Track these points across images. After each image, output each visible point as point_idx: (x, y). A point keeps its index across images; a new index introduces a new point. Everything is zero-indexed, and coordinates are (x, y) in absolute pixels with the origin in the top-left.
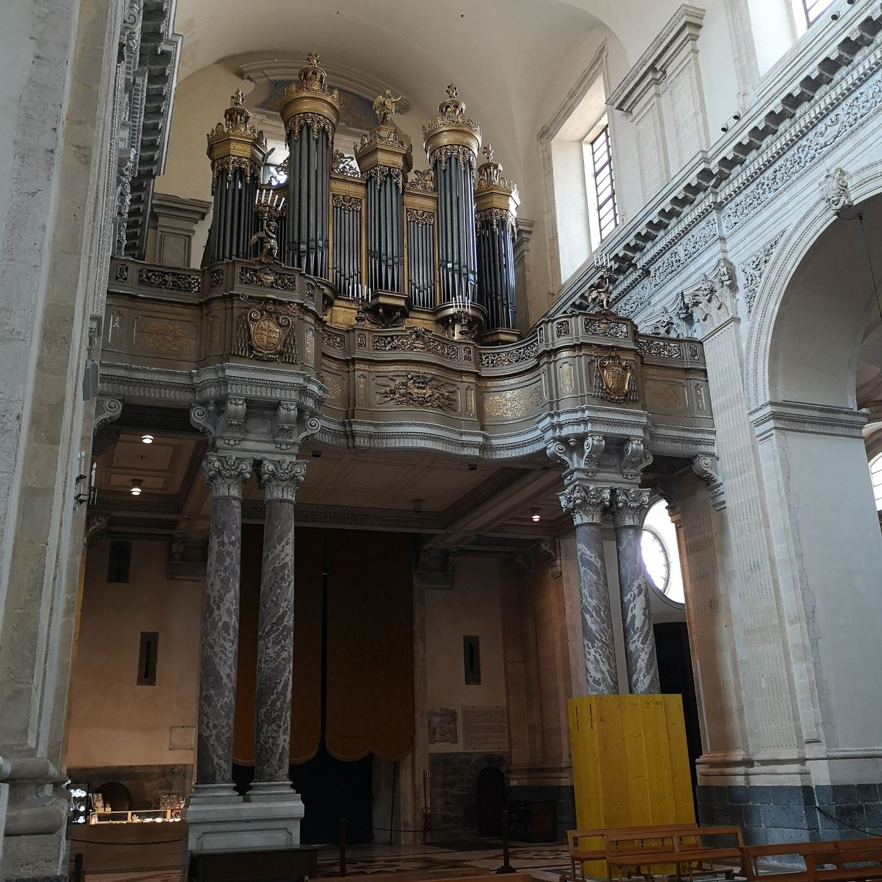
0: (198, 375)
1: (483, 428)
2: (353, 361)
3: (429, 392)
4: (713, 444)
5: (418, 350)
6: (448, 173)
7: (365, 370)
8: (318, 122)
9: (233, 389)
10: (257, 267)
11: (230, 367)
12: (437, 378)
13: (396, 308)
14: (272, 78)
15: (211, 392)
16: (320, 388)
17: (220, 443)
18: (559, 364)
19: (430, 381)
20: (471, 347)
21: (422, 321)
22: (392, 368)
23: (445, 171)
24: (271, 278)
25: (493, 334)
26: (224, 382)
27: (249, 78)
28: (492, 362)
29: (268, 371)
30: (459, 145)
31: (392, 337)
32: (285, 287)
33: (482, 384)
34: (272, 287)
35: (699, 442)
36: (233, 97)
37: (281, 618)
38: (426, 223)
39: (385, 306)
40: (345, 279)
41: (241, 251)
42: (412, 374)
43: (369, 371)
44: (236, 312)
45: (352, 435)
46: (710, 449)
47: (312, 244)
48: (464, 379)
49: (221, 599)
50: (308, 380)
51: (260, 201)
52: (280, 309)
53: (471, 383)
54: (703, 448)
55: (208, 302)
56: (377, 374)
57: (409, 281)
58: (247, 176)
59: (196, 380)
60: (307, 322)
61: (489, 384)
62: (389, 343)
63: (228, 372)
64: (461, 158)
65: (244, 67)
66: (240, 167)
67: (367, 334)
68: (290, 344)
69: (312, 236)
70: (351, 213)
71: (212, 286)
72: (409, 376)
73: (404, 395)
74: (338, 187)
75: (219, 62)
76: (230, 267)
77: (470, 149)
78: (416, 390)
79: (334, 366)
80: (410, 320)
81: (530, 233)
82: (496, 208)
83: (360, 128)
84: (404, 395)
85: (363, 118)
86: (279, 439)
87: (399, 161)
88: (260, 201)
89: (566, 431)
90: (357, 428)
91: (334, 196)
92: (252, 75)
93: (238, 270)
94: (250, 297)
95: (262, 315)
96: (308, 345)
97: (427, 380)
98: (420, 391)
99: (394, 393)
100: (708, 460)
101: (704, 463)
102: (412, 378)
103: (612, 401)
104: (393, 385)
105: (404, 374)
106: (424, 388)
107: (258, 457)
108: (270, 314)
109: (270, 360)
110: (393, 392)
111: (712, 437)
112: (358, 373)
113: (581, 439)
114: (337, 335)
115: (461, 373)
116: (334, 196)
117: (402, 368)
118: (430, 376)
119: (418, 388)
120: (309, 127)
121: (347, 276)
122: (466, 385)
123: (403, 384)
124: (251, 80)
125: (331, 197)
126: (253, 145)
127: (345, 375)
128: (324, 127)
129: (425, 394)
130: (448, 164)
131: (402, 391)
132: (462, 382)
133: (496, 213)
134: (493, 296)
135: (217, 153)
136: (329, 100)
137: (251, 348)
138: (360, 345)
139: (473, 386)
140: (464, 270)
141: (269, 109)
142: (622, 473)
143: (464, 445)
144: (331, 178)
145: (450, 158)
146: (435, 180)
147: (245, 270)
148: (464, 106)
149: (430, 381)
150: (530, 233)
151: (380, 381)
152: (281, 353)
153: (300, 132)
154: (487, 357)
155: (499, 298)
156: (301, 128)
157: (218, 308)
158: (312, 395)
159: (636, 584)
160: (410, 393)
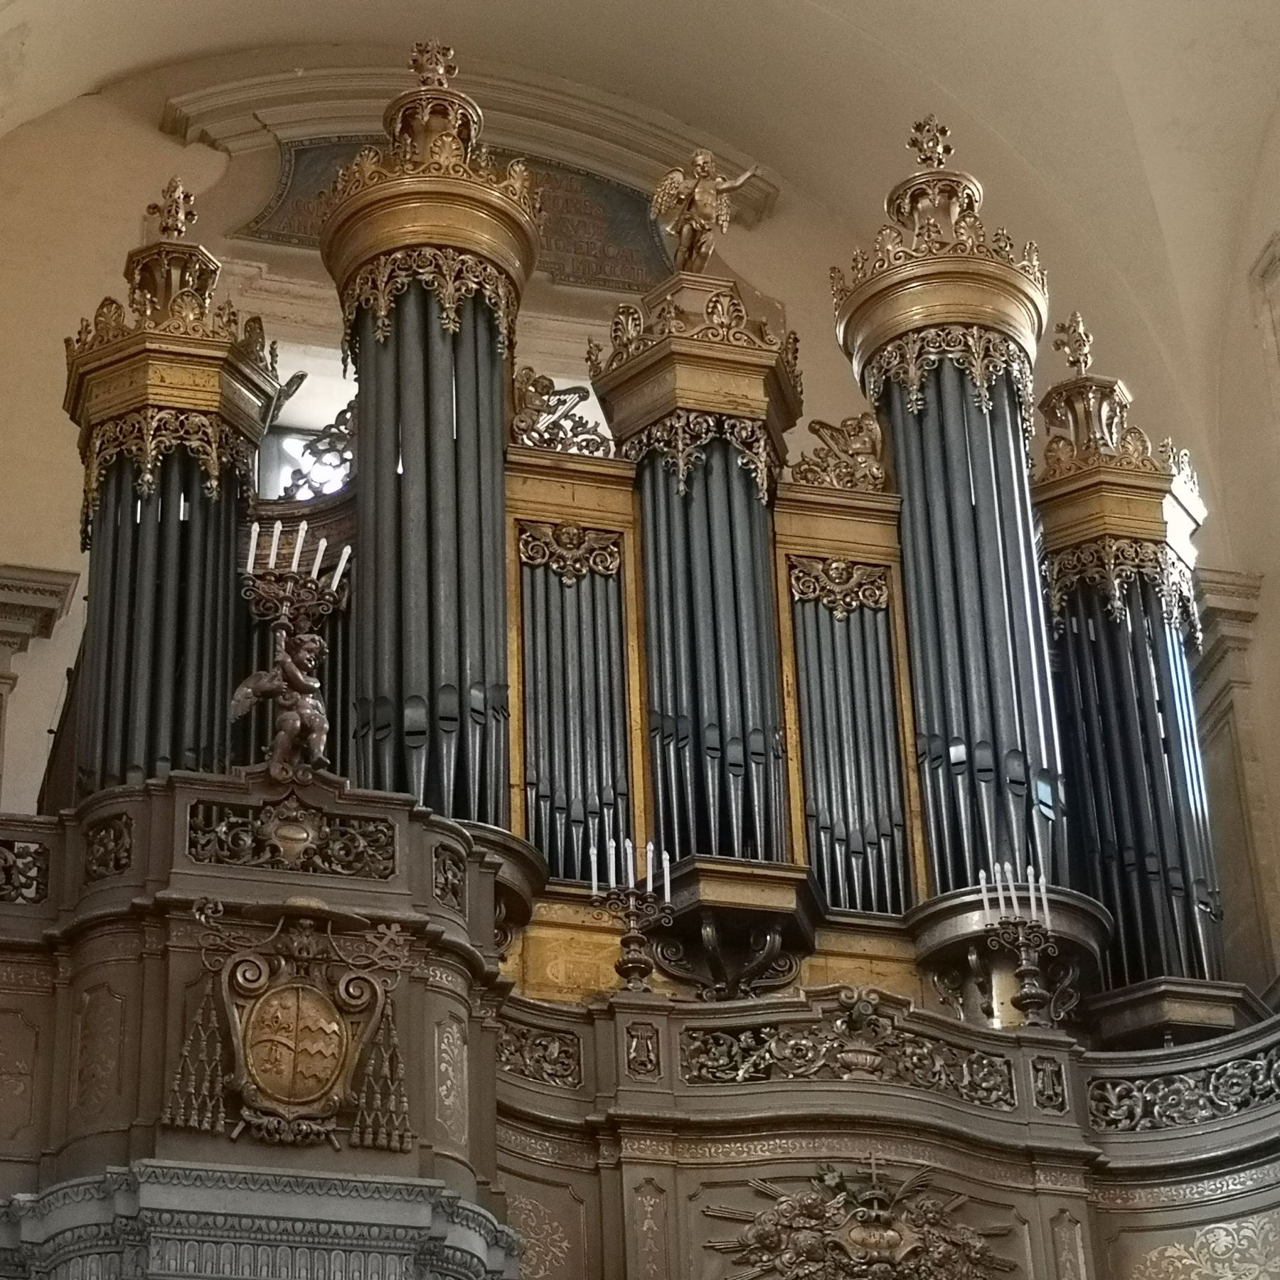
0: (38, 1211)
2: (613, 1128)
3: (910, 1240)
5: (858, 1075)
6: (931, 424)
7: (658, 1163)
8: (459, 276)
10: (256, 799)
11: (155, 1177)
12: (937, 1181)
13: (764, 919)
14: (285, 134)
16: (495, 1241)
19: (913, 1192)
20: (1063, 1058)
21: (863, 963)
22: (761, 1150)
23: (921, 416)
24: (304, 836)
25: (1134, 1005)
27: (204, 138)
28: (1148, 1112)
29: (296, 1185)
30: (968, 326)
31: (756, 1030)
32: (354, 863)
33: (1115, 1198)
34: (304, 867)
36: (154, 208)
38: (862, 606)
39: (723, 915)
40: (569, 823)
41: (188, 740)
42: (841, 1168)
43: (676, 1166)
44: (179, 967)
47: (448, 703)
48: (1044, 1181)
50: (448, 1210)
51: (261, 560)
52: (342, 947)
53: (1070, 1195)
55: (75, 938)
56: (705, 1176)
57: (808, 816)
58: (206, 476)
59: (30, 1232)
60: (438, 990)
61: (1141, 1197)
62: (746, 1052)
63: (153, 1196)
64: (977, 370)
65: (187, 103)
66: (182, 447)
67: (660, 1022)
68: (377, 1074)
69: (446, 672)
70: (585, 584)
71: (90, 877)
72: (831, 1180)
73: (811, 1256)
75: (102, 89)
76: (157, 804)
77: (1007, 338)
78: (857, 1234)
79: (542, 1150)
80: (819, 961)
81: (1247, 618)
82: (1117, 538)
83: (605, 284)
84: (811, 1256)
85: (612, 251)
87: (754, 394)
88: (261, 560)
91: (521, 527)
92: (214, 129)
93: (183, 818)
94: (232, 911)
95: (274, 972)
96: (444, 1077)
97: (899, 1193)
98: (875, 1236)
99: (774, 1249)
102: (840, 1187)
104: (767, 1216)
105: (810, 1170)
106: (888, 1225)
108: (303, 968)
109: (306, 1142)
110: (768, 1244)
112: (632, 1176)
114: (550, 1032)
115: (1031, 1157)
116: (521, 527)
117: (799, 1147)
118: (908, 1177)
119: (866, 1223)
120: (426, 296)
121: (577, 810)
122: (1050, 1207)
123: (809, 1211)
124: (213, 144)
125: (511, 533)
126: (230, 367)
127: (584, 1185)
128: (479, 293)
129: (892, 1246)
130: (931, 393)
131: (805, 1238)
132: (1035, 1193)
133: (1120, 556)
134: (1130, 857)
135: (101, 402)
136: (495, 196)
137: (235, 1100)
138: (636, 1066)
139: (1078, 1209)
140: (1014, 769)
141: (277, 238)
144: (508, 465)
145: (937, 372)
146: (887, 451)
147: (205, 815)
148: (976, 189)
149: (913, 1192)
150: (1247, 618)
151: (720, 1202)
152: (345, 1113)
153: (396, 314)
154: (1127, 1094)
155: (1152, 864)
156: (399, 299)
160: (837, 1246)
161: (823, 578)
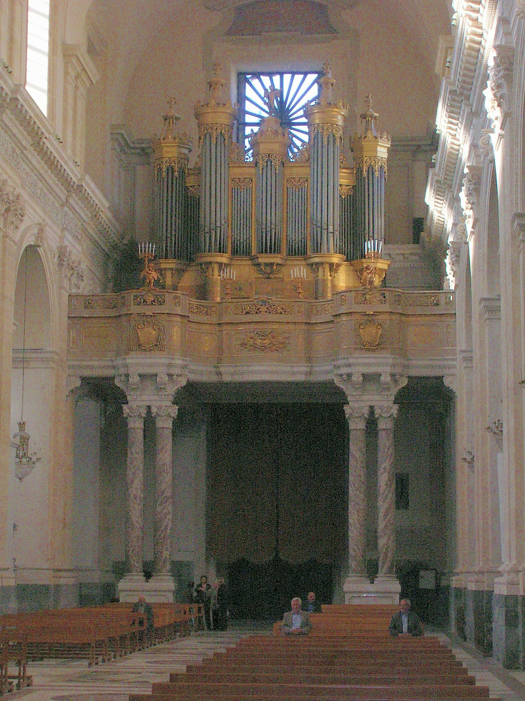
1: (309, 359)
4: (454, 367)
9: (131, 370)
15: (122, 371)
17: (129, 398)
18: (341, 323)
26: (126, 366)
35: (445, 367)
37: (163, 492)
45: (220, 374)
46: (453, 371)
49: (132, 482)
54: (446, 372)
74: (236, 172)
86: (161, 393)
89: (344, 371)
90: (222, 369)
100: (450, 379)
101: (447, 382)
103: (368, 350)
107: (148, 403)
111: (454, 363)
113: (349, 375)
114: (213, 307)
130: (316, 139)
142: (380, 395)
143: (294, 373)
147: (136, 297)
157: (124, 318)
158: (176, 366)
159: (383, 466)
161: (294, 183)
